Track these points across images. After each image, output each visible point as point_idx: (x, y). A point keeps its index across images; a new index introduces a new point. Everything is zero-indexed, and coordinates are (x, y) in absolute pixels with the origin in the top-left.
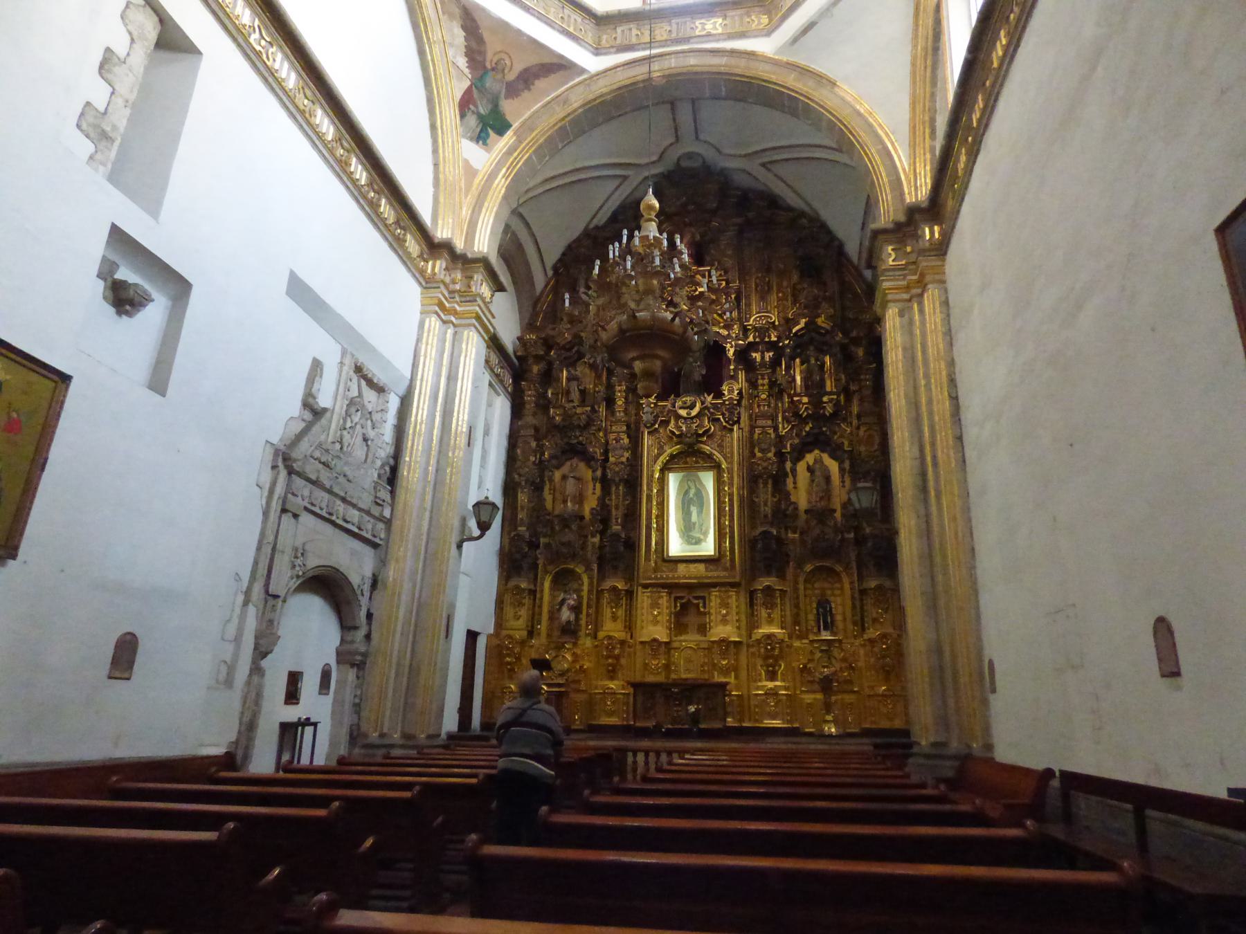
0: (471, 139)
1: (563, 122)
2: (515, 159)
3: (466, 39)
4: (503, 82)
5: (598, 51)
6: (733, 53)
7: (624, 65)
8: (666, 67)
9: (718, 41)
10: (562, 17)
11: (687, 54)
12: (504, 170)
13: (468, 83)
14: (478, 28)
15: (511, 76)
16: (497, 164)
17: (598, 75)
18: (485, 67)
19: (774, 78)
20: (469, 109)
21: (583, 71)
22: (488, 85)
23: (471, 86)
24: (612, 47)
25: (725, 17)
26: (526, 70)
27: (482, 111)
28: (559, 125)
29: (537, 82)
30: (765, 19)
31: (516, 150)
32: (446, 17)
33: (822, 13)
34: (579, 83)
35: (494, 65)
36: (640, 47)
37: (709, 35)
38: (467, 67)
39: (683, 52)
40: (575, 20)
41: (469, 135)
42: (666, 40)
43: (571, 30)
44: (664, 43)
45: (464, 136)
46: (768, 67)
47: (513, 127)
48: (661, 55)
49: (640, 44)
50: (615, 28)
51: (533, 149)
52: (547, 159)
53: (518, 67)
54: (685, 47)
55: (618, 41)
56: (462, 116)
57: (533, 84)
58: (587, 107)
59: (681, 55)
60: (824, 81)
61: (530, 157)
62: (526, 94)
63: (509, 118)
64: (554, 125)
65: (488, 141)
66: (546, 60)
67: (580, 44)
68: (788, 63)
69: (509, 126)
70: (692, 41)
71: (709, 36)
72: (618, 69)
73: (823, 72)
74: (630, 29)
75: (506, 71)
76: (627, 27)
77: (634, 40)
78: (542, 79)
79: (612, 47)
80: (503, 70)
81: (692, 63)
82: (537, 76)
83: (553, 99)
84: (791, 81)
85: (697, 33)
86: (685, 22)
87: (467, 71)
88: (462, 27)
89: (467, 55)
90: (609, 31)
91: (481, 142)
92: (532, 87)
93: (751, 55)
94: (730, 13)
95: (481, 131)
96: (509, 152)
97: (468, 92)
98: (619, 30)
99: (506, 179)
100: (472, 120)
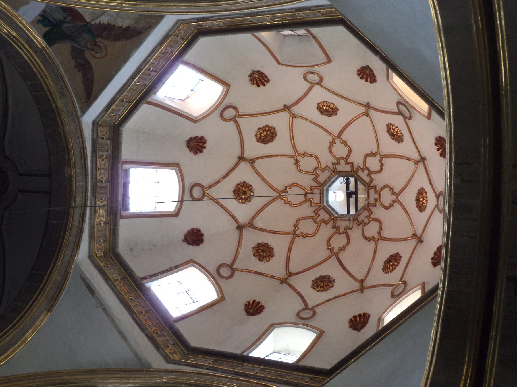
0: (44, 11)
1: (46, 90)
2: (23, 45)
3: (120, 28)
4: (84, 47)
5: (95, 124)
6: (81, 231)
7: (83, 144)
8: (78, 178)
9: (90, 219)
10: (123, 101)
11: (84, 195)
12: (14, 34)
13: (88, 20)
14: (127, 38)
15: (88, 54)
16: (20, 27)
17: (79, 123)
18: (98, 36)
19: (59, 264)
20: (69, 16)
21: (84, 112)
22: (85, 36)
23: (87, 23)
24: (97, 136)
25: (105, 223)
26: (91, 67)
27: (66, 25)
28: (45, 87)
29: (80, 74)
30: (100, 254)
31: (30, 46)
32: (137, 16)
33: (99, 300)
34: (74, 107)
35: (98, 43)
36: (94, 158)
37: (95, 212)
38: (100, 22)
39: (86, 192)
40: (120, 110)
41: (48, 10)
42: (96, 179)
43: (114, 107)
44: (94, 177)
45: (47, 5)
46: (67, 258)
47: (49, 48)
48: (86, 175)
49: (96, 157)
50: (110, 139)
51: (29, 62)
52: (19, 70)
53: (93, 62)
54: (89, 194)
55: (100, 141)
56: (65, 9)
57: (79, 71)
58: (55, 110)
59: (84, 190)
60: (52, 303)
61: (22, 57)
62: (73, 63)
63: (57, 45)
64: (45, 82)
65: (40, 25)
66: (96, 86)
67: (102, 112)
68: (68, 273)
69: (50, 44)
70: (93, 199)
71: (94, 212)
72: (81, 140)
73: (59, 302)
74: (107, 151)
75: (92, 52)
76: (109, 149)
77: (99, 153)
78: (82, 79)
79: (97, 136)
80: (93, 50)
81: (77, 199)
82: (84, 76)
83: (65, 84)
84: (56, 277)
85: (98, 203)
86: (106, 194)
87: (97, 21)
88: (129, 27)
89: (109, 25)
90: (108, 134)
91: (41, 18)
92: (78, 69)
93: (77, 245)
94: (108, 227)
95: (50, 21)
96: (30, 42)
97: (82, 19)
98: (108, 142)
99: (6, 34)
100: (59, 16)
